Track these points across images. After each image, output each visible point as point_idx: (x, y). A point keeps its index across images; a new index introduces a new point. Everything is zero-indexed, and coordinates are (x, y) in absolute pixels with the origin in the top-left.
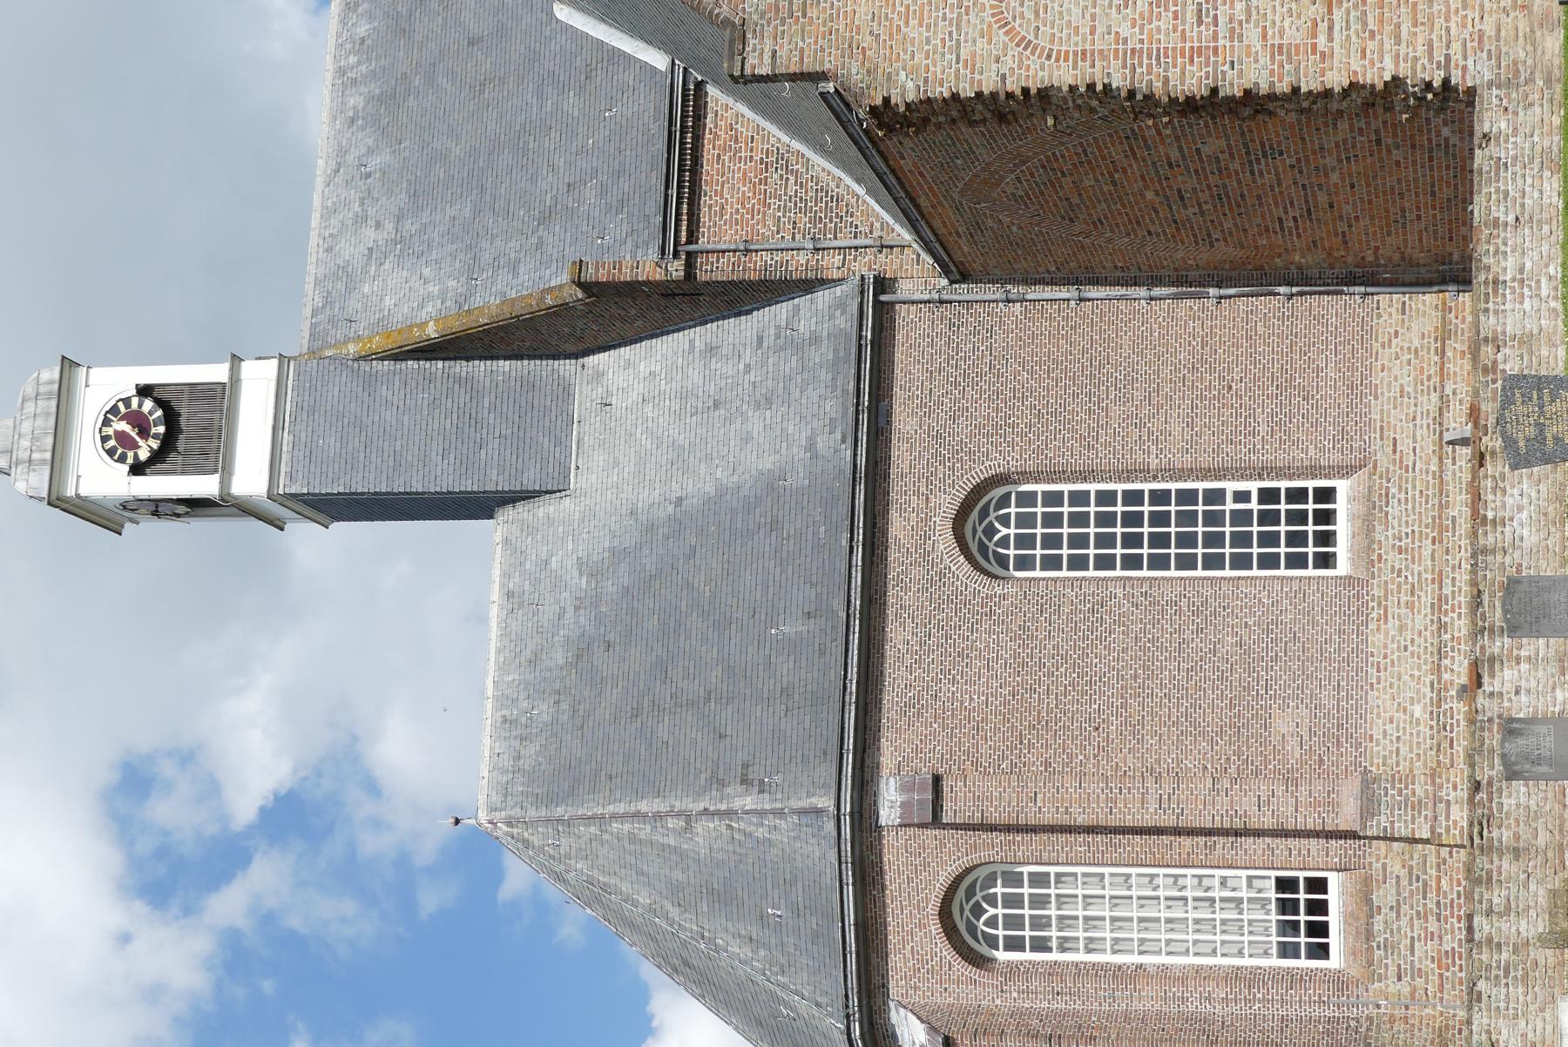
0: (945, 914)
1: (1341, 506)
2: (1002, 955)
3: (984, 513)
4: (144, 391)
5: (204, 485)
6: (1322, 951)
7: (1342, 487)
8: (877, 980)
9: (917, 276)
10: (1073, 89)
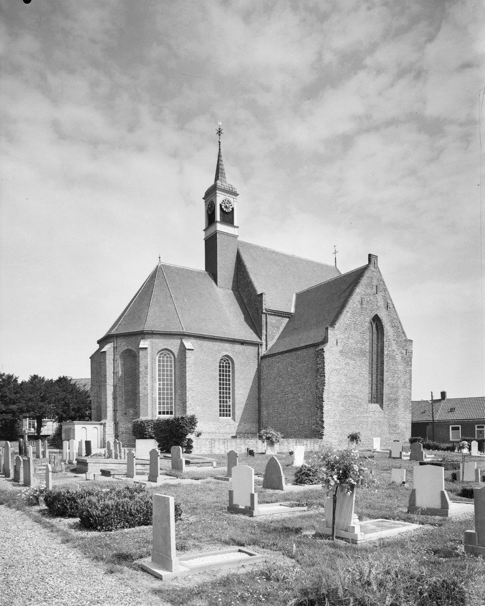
1: (228, 418)
2: (157, 358)
3: (227, 360)
4: (233, 209)
5: (218, 218)
6: (160, 413)
7: (231, 418)
8: (154, 336)
9: (263, 351)
10: (325, 380)
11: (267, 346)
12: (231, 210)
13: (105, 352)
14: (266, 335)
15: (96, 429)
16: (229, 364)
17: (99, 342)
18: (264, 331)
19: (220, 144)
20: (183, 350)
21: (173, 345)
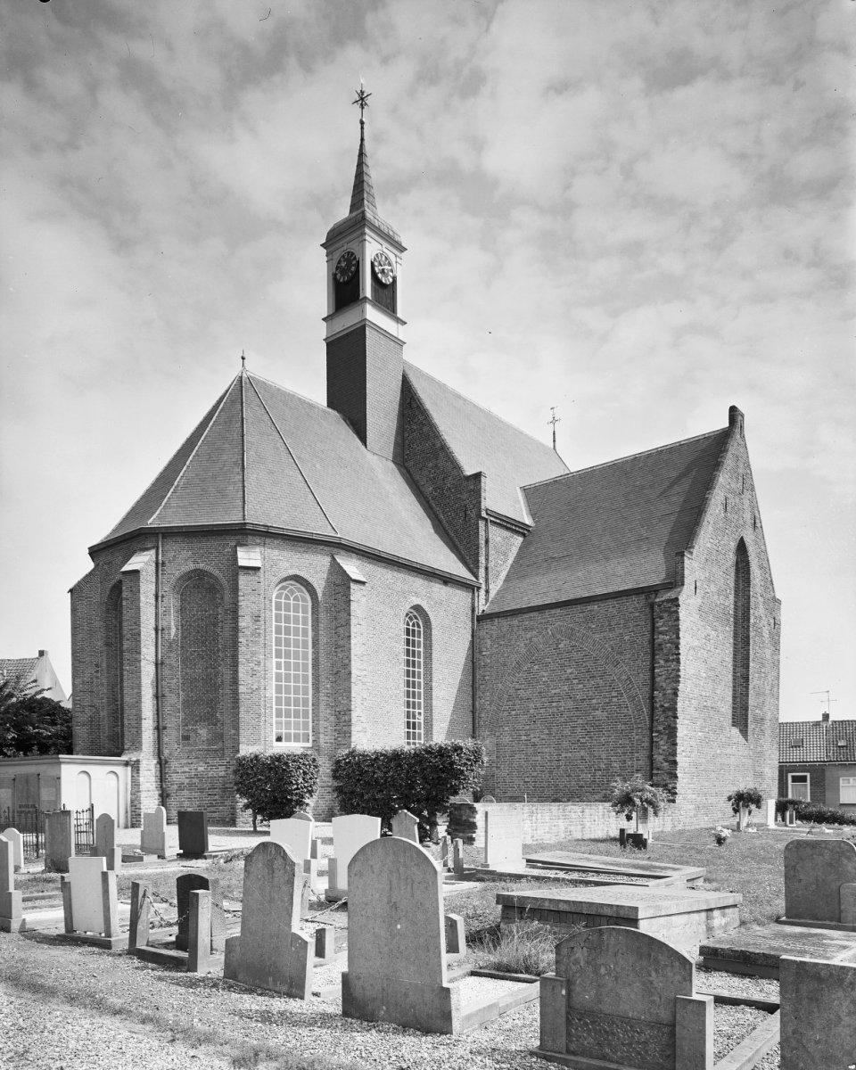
0: (297, 578)
3: (416, 618)
4: (394, 279)
9: (482, 606)
11: (487, 592)
12: (391, 280)
13: (136, 572)
14: (487, 568)
15: (114, 777)
16: (419, 627)
17: (94, 552)
18: (482, 559)
19: (362, 128)
20: (341, 583)
21: (315, 567)
